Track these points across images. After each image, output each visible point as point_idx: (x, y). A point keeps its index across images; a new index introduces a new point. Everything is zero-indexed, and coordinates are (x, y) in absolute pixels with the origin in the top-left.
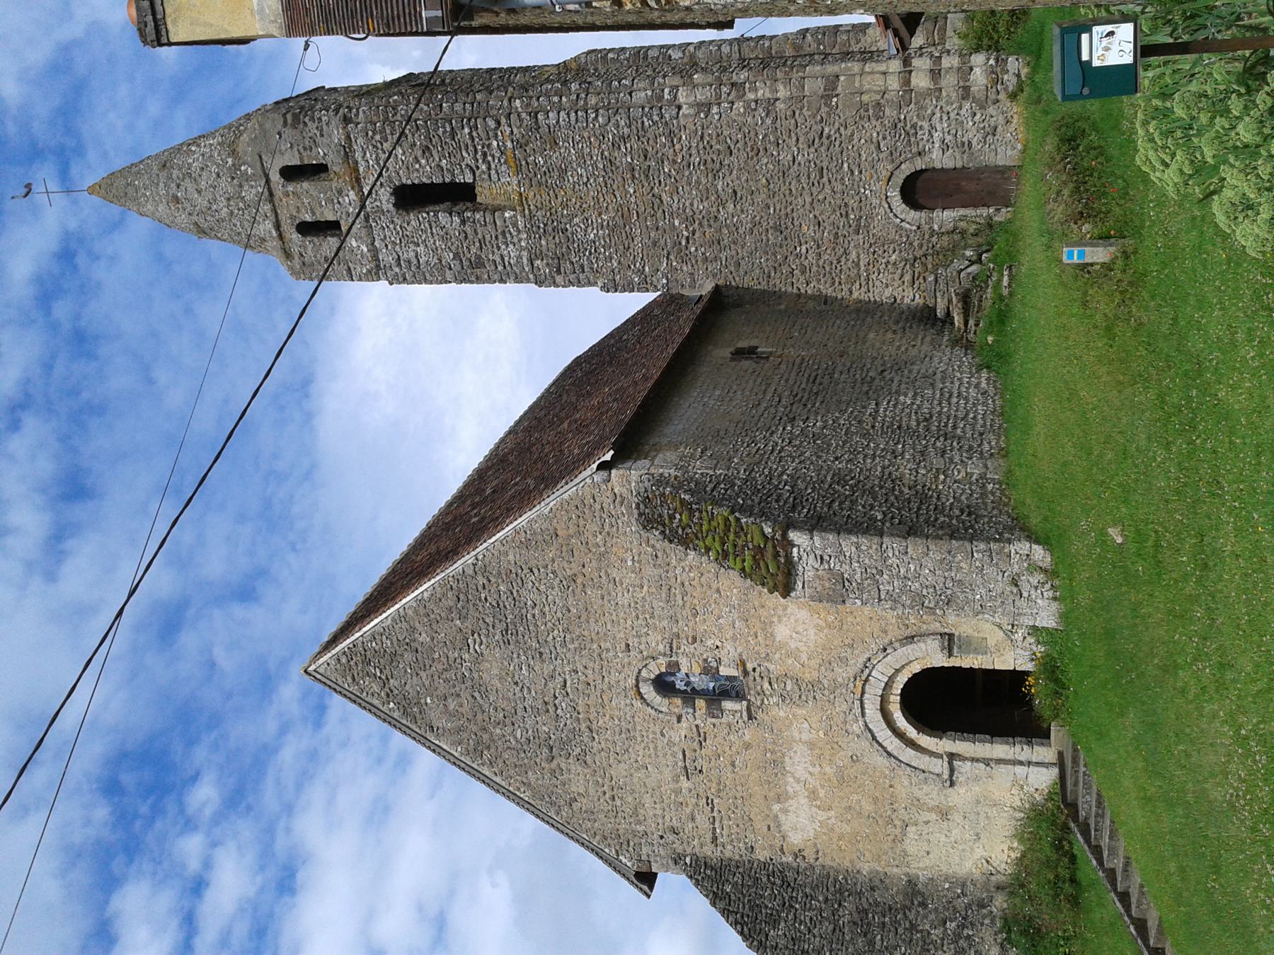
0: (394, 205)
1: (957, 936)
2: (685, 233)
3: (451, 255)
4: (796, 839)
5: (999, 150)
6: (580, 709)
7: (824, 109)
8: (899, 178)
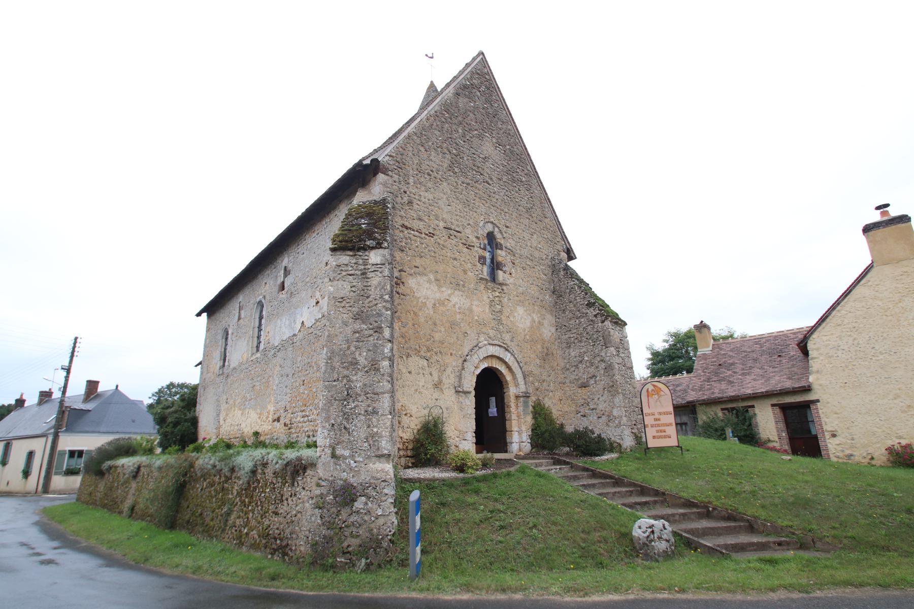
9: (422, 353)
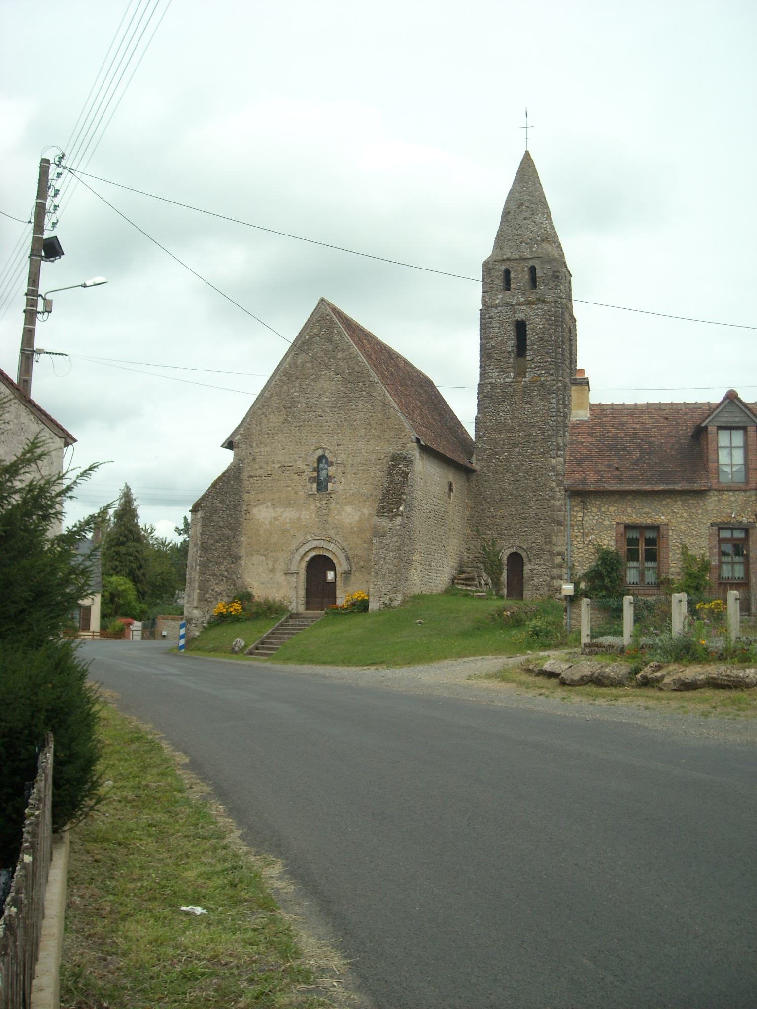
1: (223, 576)
2: (501, 458)
3: (494, 344)
4: (255, 511)
6: (309, 423)
7: (550, 521)
8: (520, 551)
9: (262, 552)
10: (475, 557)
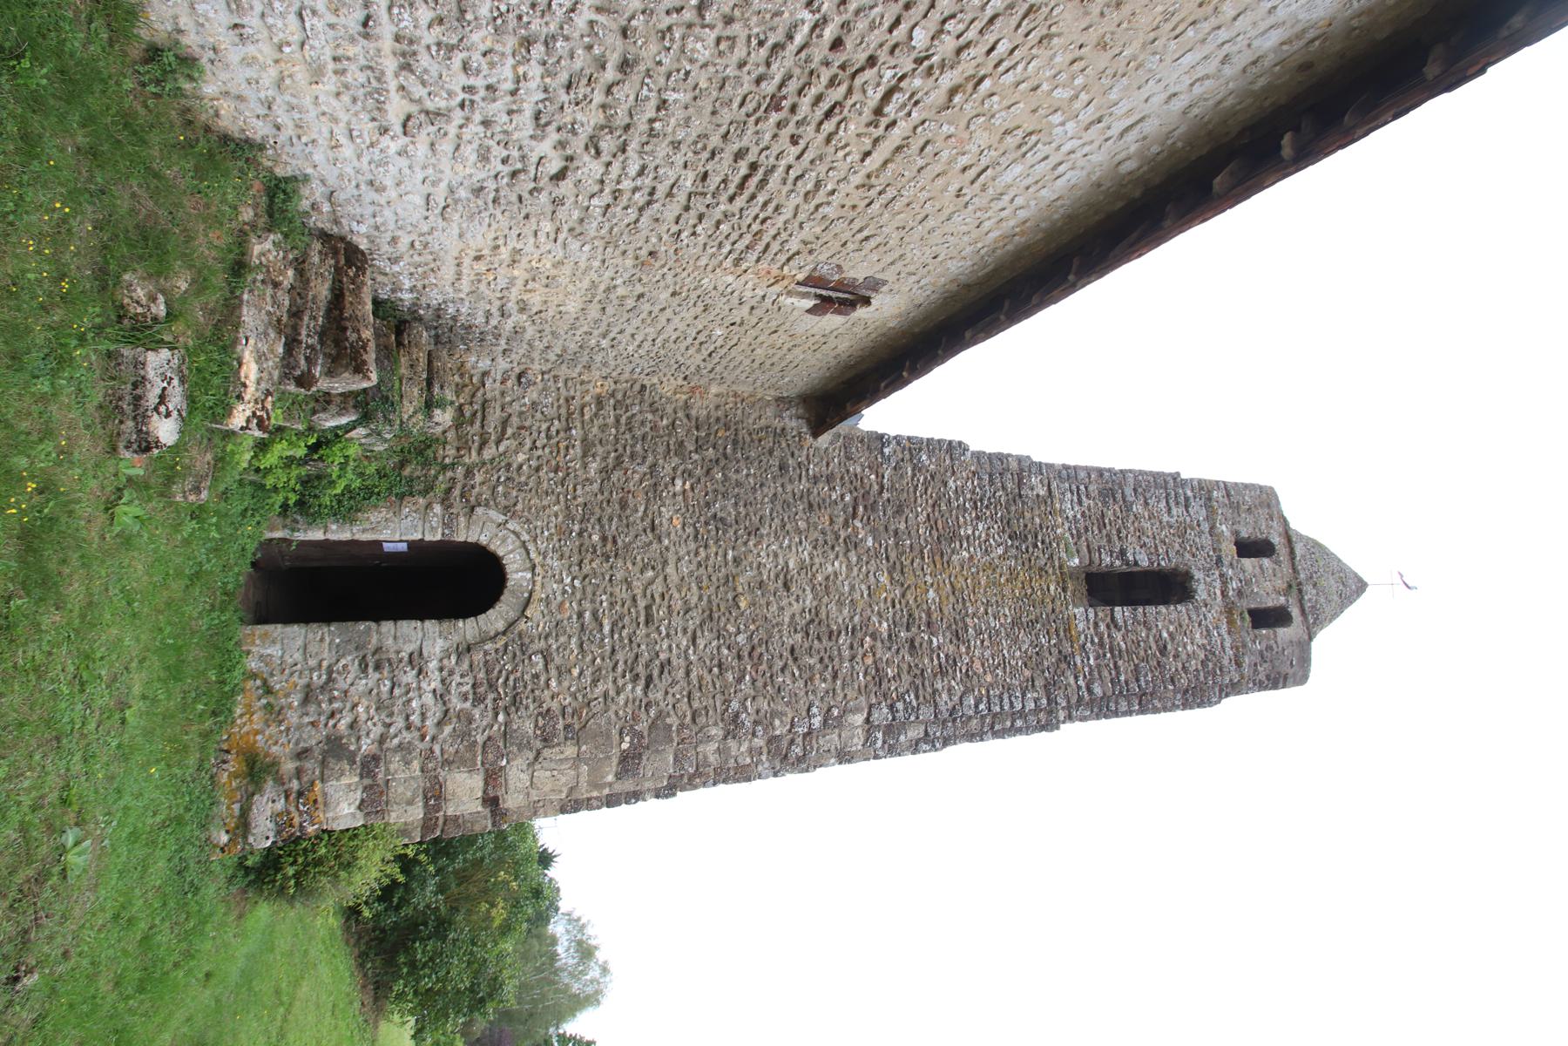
0: (1192, 578)
2: (859, 524)
5: (298, 656)
10: (485, 402)
